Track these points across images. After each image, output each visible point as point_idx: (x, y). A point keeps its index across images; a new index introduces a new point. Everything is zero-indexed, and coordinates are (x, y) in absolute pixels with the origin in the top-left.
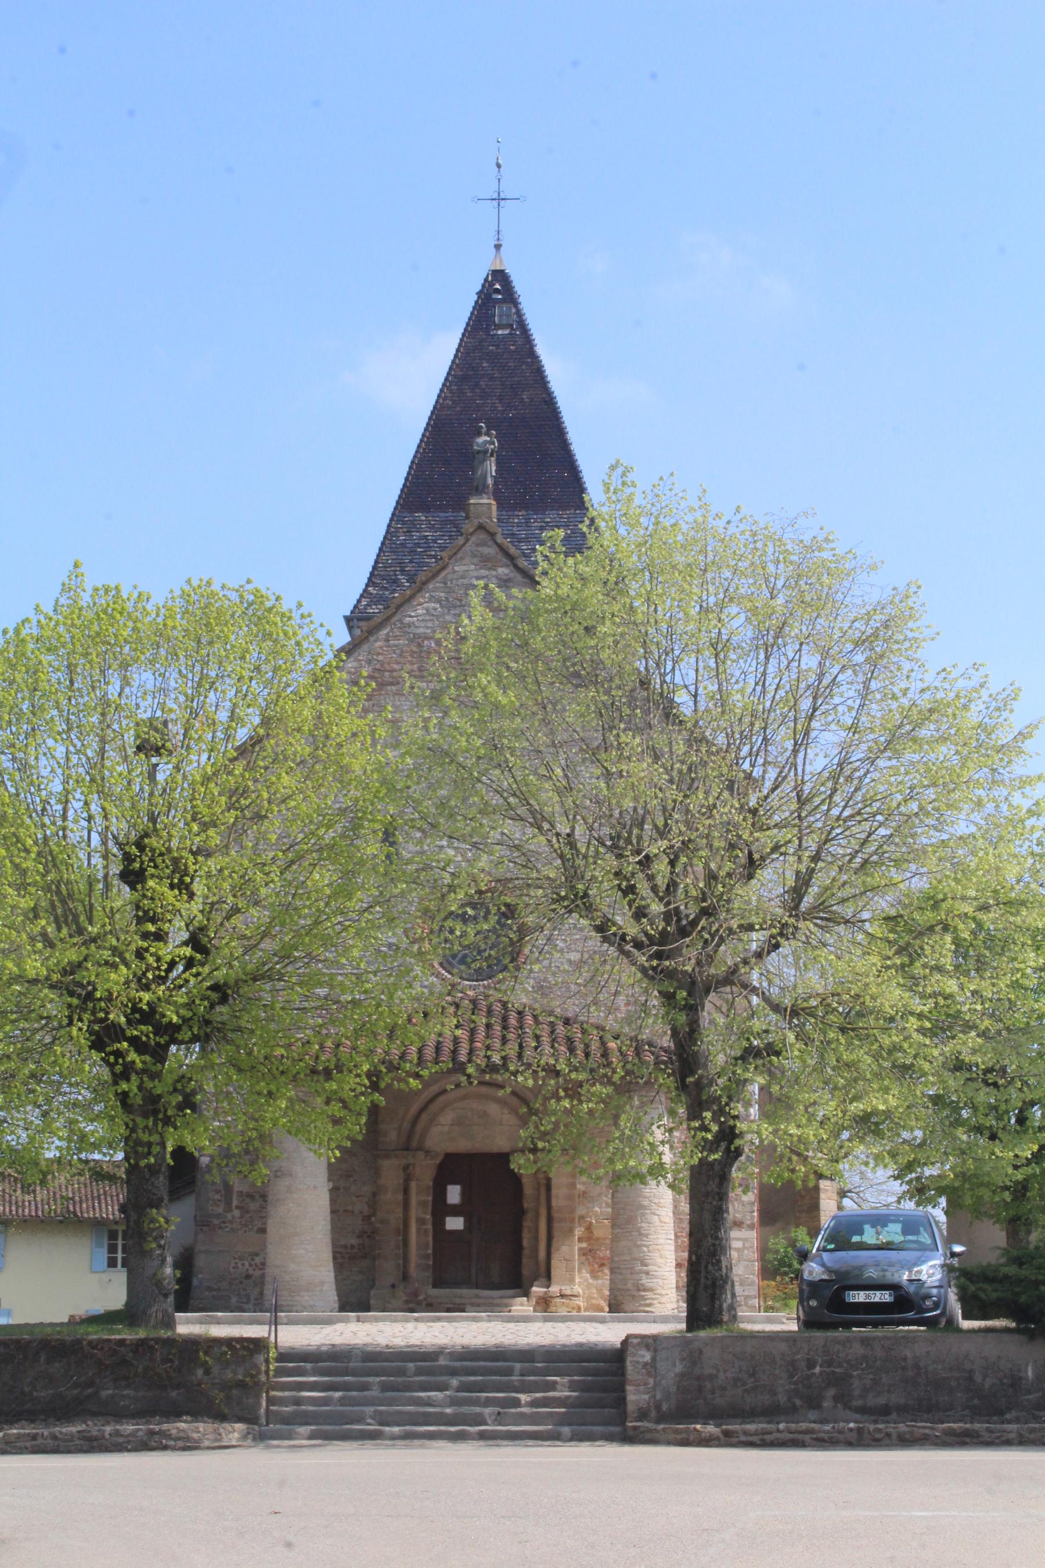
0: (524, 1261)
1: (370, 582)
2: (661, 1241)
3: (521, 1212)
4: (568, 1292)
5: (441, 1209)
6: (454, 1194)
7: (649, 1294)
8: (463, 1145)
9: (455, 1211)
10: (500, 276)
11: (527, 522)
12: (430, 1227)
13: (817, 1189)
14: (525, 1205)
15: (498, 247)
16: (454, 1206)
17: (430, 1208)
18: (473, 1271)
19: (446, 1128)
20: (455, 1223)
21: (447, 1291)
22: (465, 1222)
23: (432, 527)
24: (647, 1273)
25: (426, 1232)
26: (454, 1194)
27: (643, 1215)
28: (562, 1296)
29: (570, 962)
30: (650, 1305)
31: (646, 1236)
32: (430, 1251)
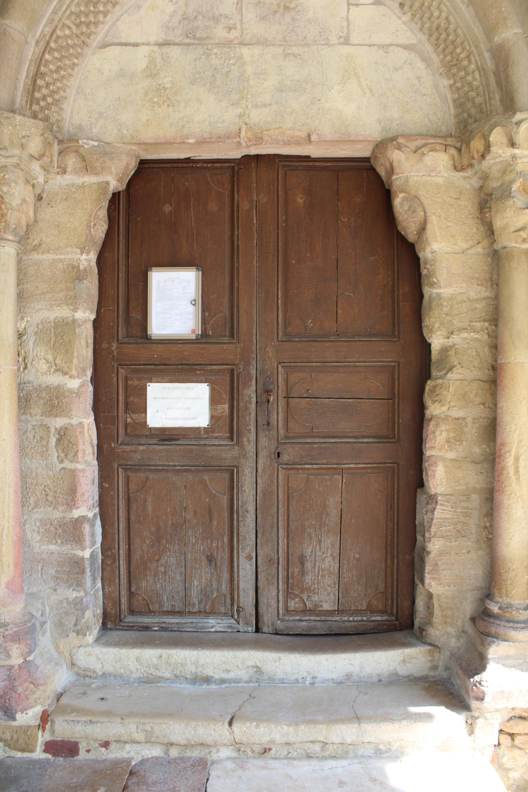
0: (435, 546)
3: (421, 366)
5: (124, 353)
6: (174, 302)
8: (205, 121)
9: (177, 362)
12: (84, 422)
14: (437, 342)
17: (84, 351)
18: (246, 570)
19: (139, 59)
20: (178, 405)
21: (150, 655)
22: (214, 401)
25: (65, 439)
26: (174, 302)
32: (87, 507)
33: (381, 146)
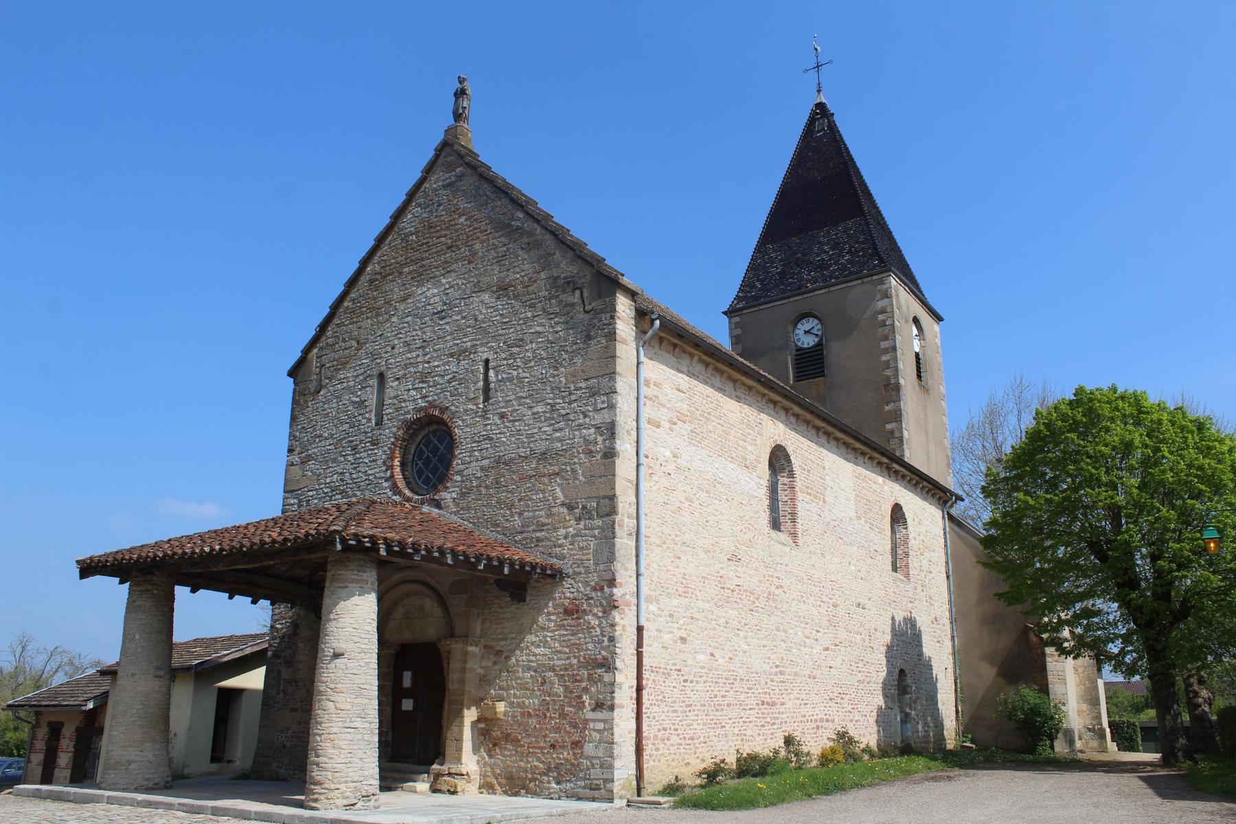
1: (741, 290)
2: (334, 730)
4: (453, 771)
6: (407, 679)
7: (317, 789)
9: (408, 694)
10: (821, 106)
11: (829, 232)
13: (1044, 654)
15: (819, 91)
16: (407, 689)
23: (776, 251)
24: (317, 765)
26: (407, 679)
27: (320, 701)
28: (450, 774)
29: (482, 469)
30: (316, 800)
31: (320, 723)
33: (439, 640)
